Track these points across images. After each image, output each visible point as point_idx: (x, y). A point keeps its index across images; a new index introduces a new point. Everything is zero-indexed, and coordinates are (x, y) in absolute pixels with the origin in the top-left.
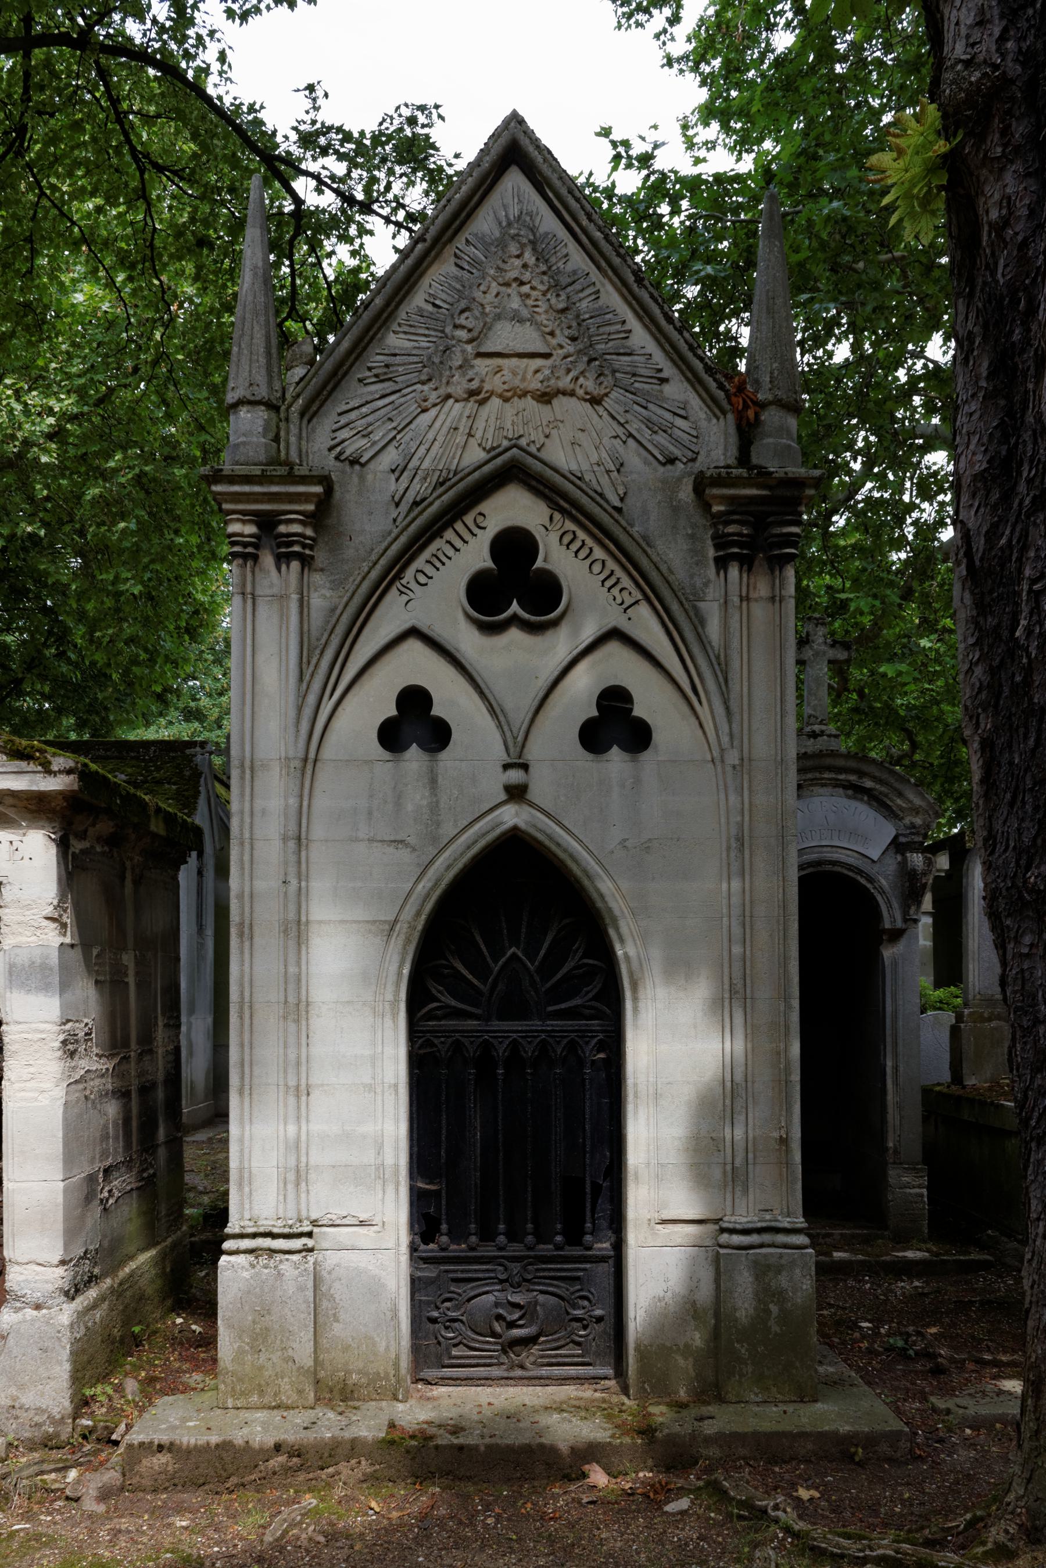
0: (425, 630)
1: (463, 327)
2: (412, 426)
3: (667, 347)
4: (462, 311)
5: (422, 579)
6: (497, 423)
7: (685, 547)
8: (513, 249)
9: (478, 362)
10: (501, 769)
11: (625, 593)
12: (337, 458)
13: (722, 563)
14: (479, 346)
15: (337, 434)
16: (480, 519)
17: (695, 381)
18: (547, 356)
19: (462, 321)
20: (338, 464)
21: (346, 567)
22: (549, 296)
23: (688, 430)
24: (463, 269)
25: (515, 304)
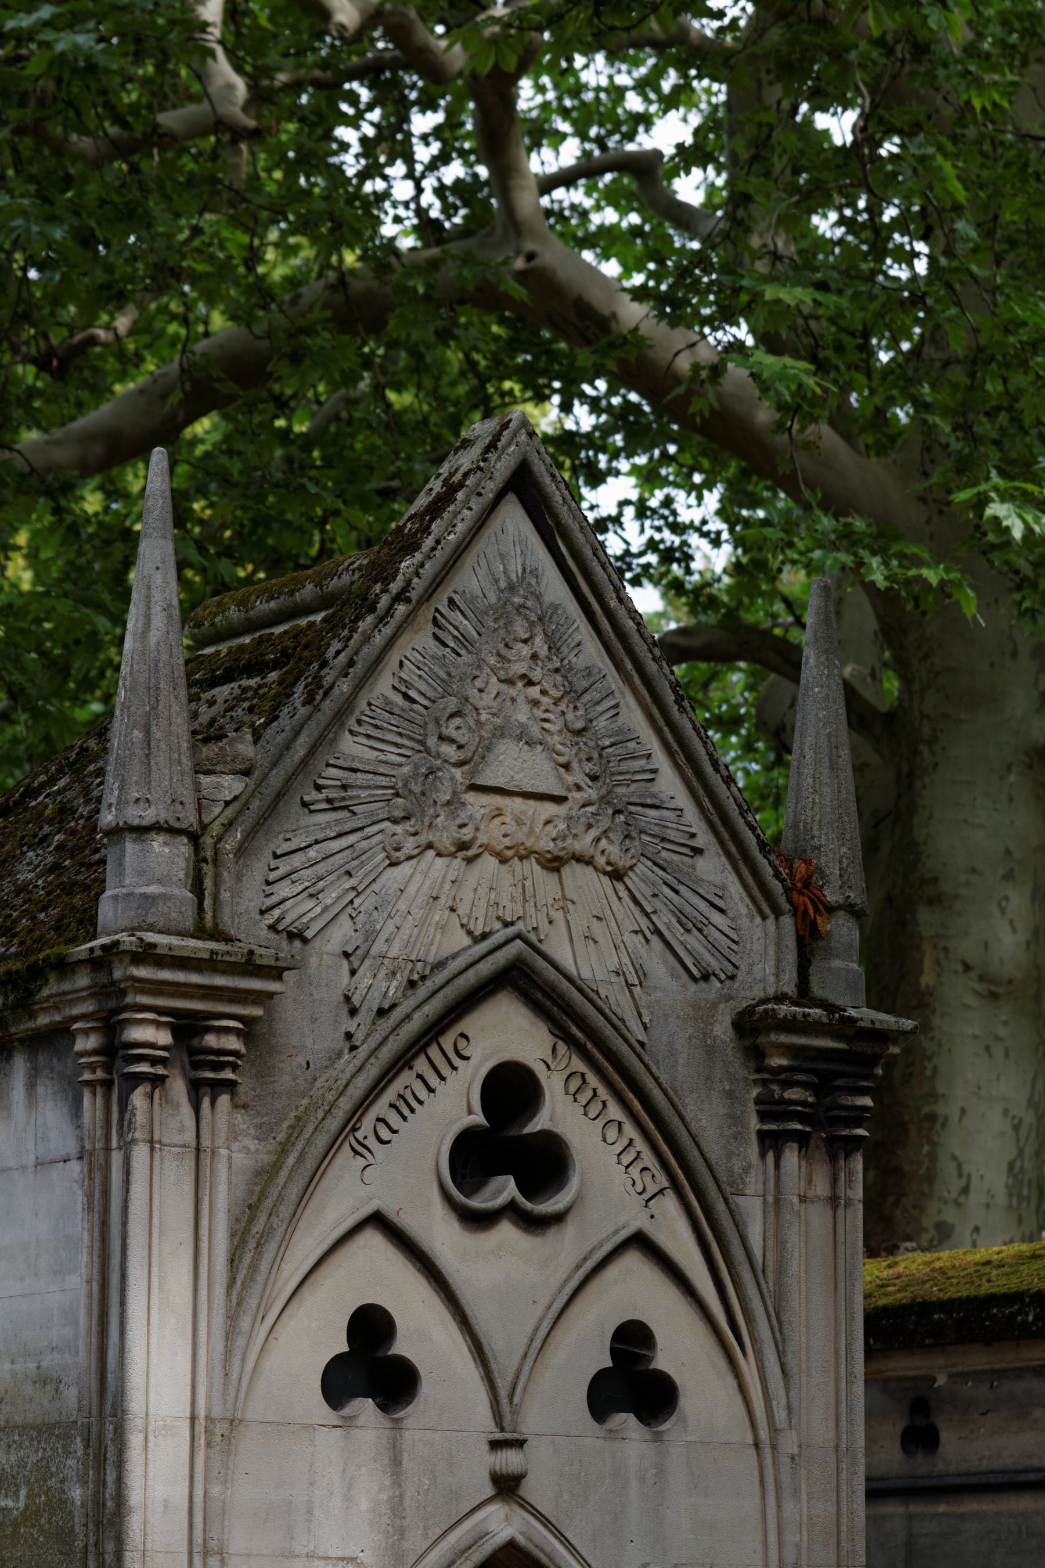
0: (393, 1217)
1: (452, 741)
2: (376, 887)
3: (706, 802)
4: (452, 716)
5: (385, 1134)
6: (490, 891)
7: (722, 1111)
8: (520, 629)
9: (470, 797)
10: (486, 1447)
11: (647, 1176)
12: (272, 927)
13: (771, 1142)
14: (474, 773)
15: (275, 888)
16: (462, 1043)
17: (739, 857)
18: (560, 800)
19: (450, 731)
20: (272, 936)
21: (277, 1105)
22: (563, 706)
23: (728, 931)
24: (445, 645)
25: (522, 715)
